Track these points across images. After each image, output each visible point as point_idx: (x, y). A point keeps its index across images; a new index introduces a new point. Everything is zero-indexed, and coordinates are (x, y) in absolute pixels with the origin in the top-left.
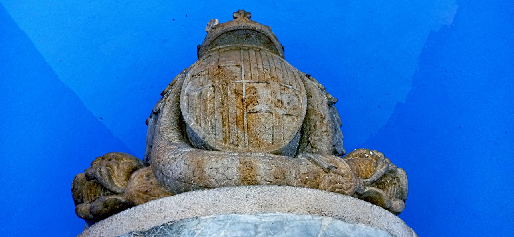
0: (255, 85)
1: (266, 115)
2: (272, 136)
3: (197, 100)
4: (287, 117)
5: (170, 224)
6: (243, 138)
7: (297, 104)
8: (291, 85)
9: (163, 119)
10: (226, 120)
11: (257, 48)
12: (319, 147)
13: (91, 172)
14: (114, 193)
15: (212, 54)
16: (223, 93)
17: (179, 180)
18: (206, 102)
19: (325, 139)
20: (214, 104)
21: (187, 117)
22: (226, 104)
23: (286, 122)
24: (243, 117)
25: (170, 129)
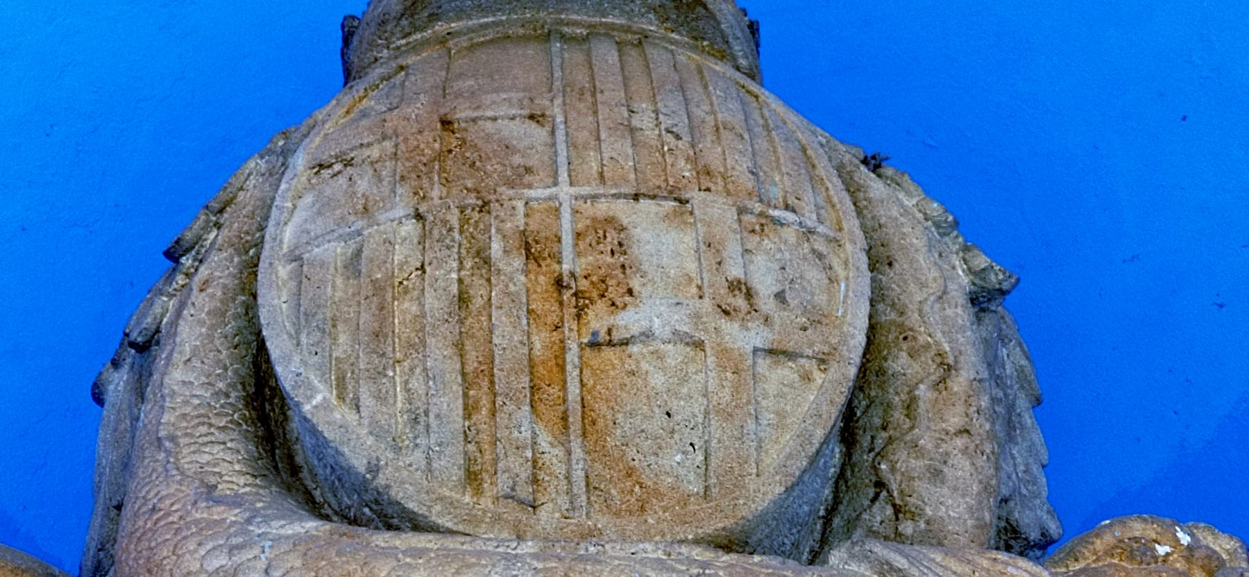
0: (622, 210)
1: (675, 354)
2: (700, 458)
3: (339, 281)
4: (777, 363)
6: (560, 469)
7: (821, 299)
8: (794, 211)
9: (177, 375)
11: (628, 30)
12: (929, 511)
15: (410, 60)
16: (464, 251)
19: (961, 469)
20: (422, 305)
22: (478, 302)
23: (772, 388)
24: (562, 368)
25: (211, 425)
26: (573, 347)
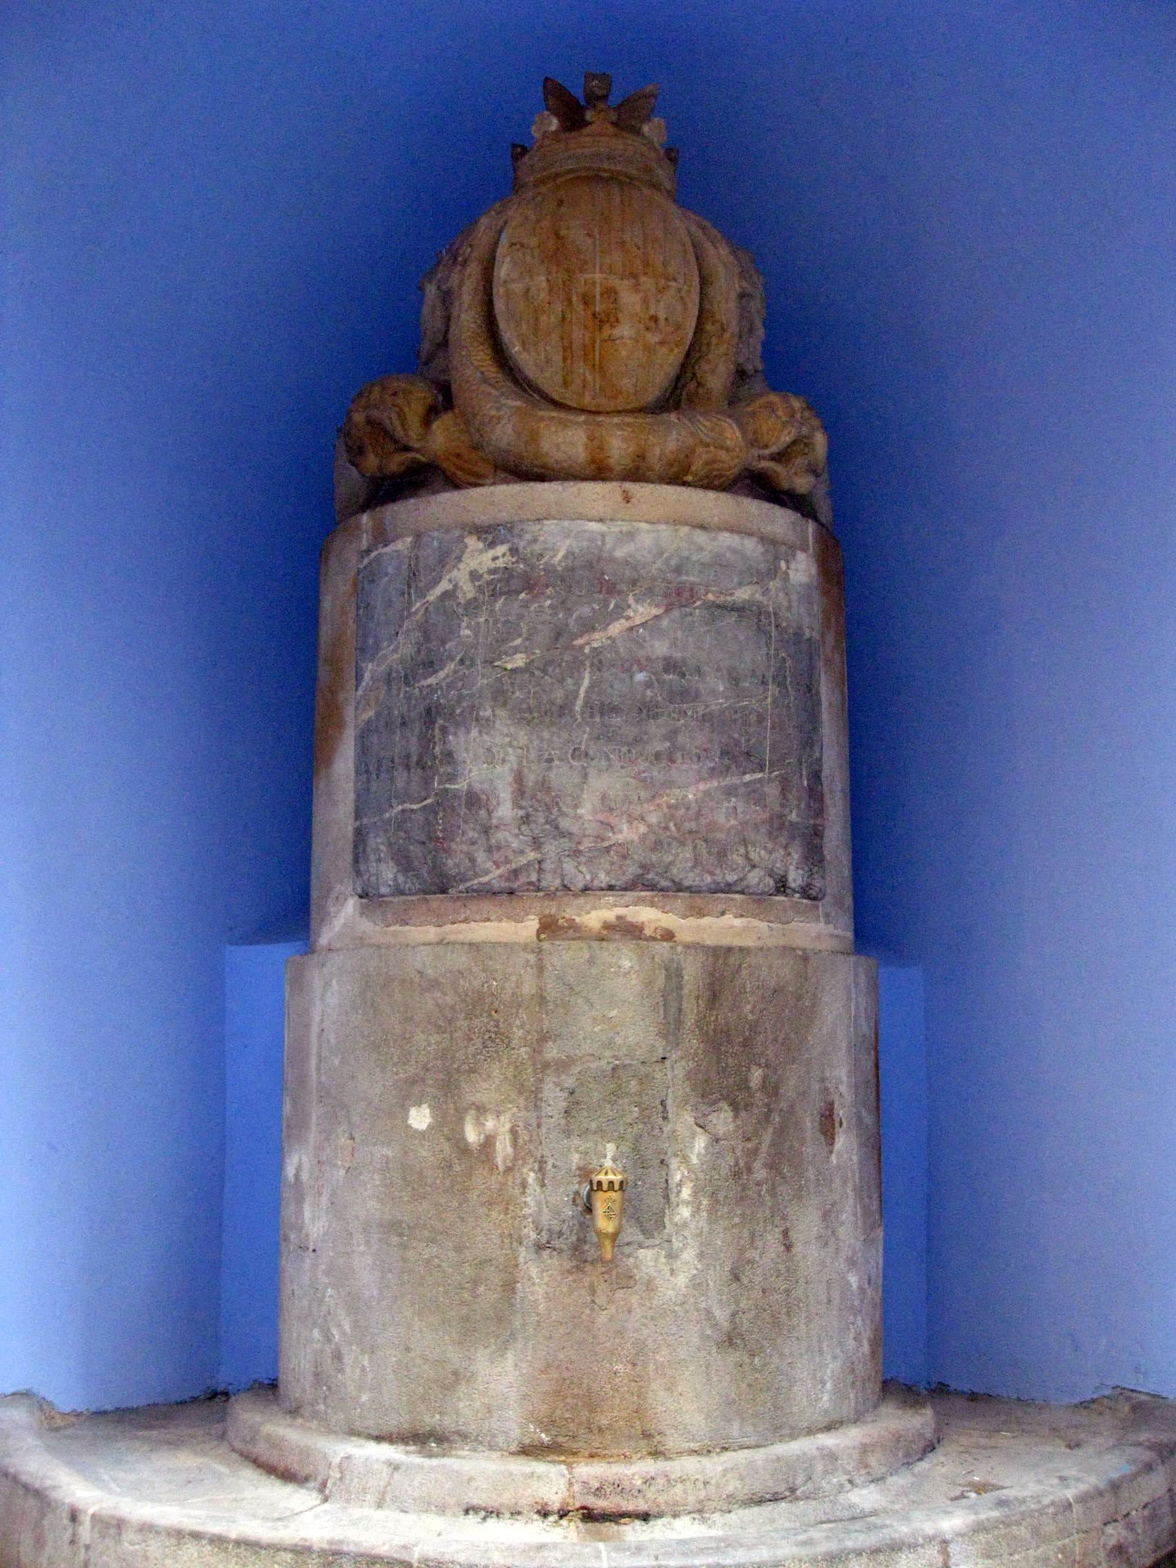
5: (509, 525)
10: (567, 349)
13: (375, 414)
14: (406, 449)
17: (507, 452)
18: (538, 312)
24: (594, 347)
26: (598, 341)
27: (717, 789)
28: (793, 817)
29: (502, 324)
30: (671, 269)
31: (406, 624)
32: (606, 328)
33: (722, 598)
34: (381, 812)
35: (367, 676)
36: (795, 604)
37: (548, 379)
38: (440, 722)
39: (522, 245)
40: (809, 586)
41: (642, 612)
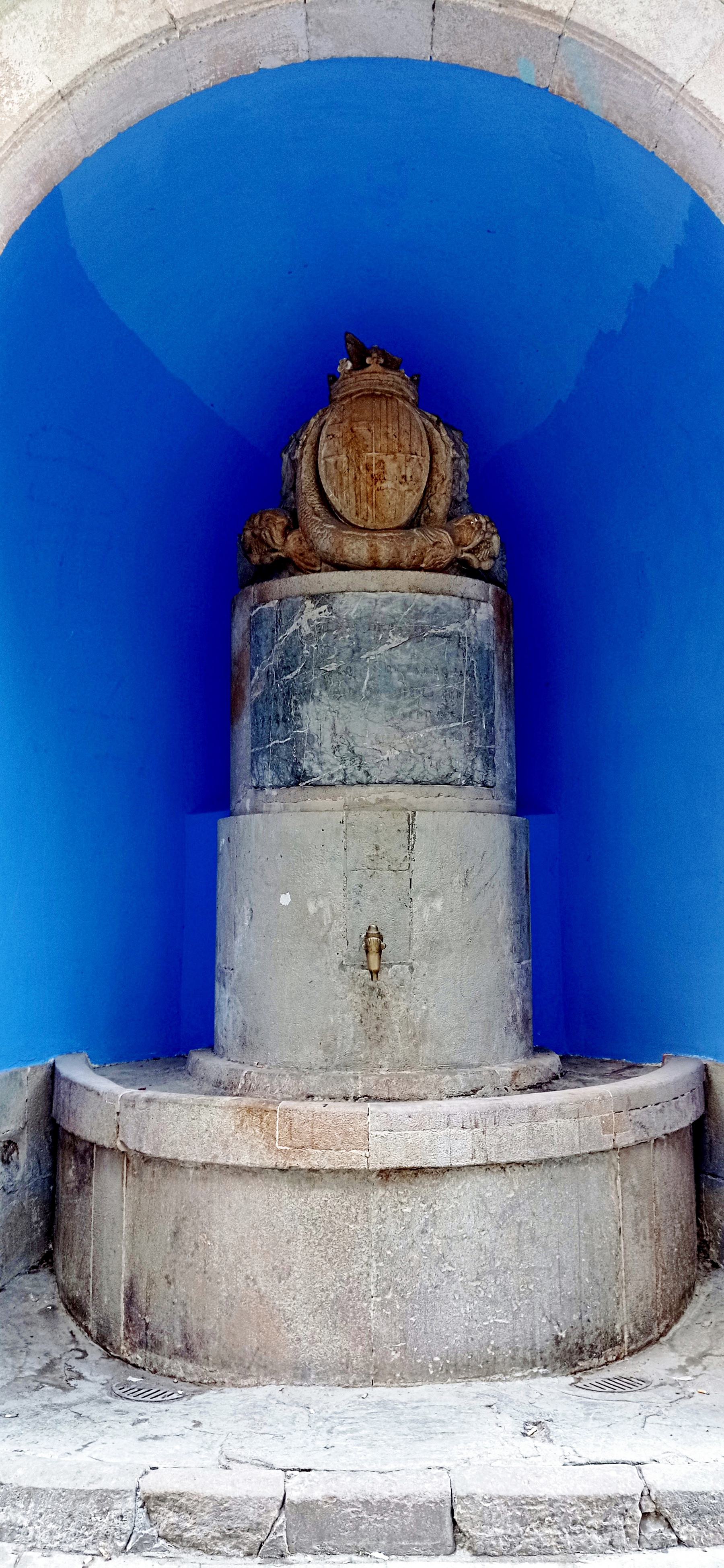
9: (303, 475)
21: (326, 488)
27: (436, 731)
28: (477, 745)
29: (323, 481)
30: (414, 449)
31: (276, 647)
32: (378, 483)
33: (439, 631)
34: (265, 744)
35: (256, 674)
36: (479, 632)
37: (349, 514)
38: (294, 698)
39: (333, 436)
40: (488, 621)
41: (395, 640)
